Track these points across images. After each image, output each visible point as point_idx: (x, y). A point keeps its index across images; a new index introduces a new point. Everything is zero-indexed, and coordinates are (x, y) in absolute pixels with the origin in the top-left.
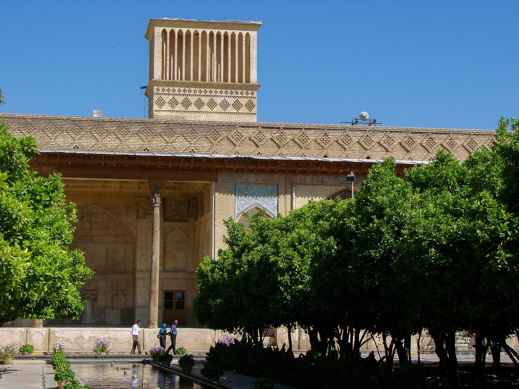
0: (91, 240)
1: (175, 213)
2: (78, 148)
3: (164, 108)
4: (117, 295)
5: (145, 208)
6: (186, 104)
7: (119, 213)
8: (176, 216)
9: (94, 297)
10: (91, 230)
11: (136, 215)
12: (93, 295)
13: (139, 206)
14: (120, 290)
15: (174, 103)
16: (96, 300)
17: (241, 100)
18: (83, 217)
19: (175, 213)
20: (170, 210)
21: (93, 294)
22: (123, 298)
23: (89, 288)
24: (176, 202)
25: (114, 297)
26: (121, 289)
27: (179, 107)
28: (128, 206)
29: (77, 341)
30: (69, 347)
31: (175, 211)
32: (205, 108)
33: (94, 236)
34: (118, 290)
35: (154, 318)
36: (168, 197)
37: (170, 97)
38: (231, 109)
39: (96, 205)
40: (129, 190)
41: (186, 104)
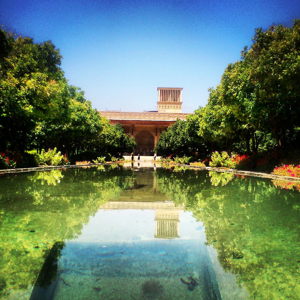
3: (161, 108)
6: (165, 107)
15: (163, 107)
16: (146, 151)
17: (178, 106)
27: (164, 108)
32: (170, 108)
37: (162, 105)
38: (176, 108)
41: (165, 107)
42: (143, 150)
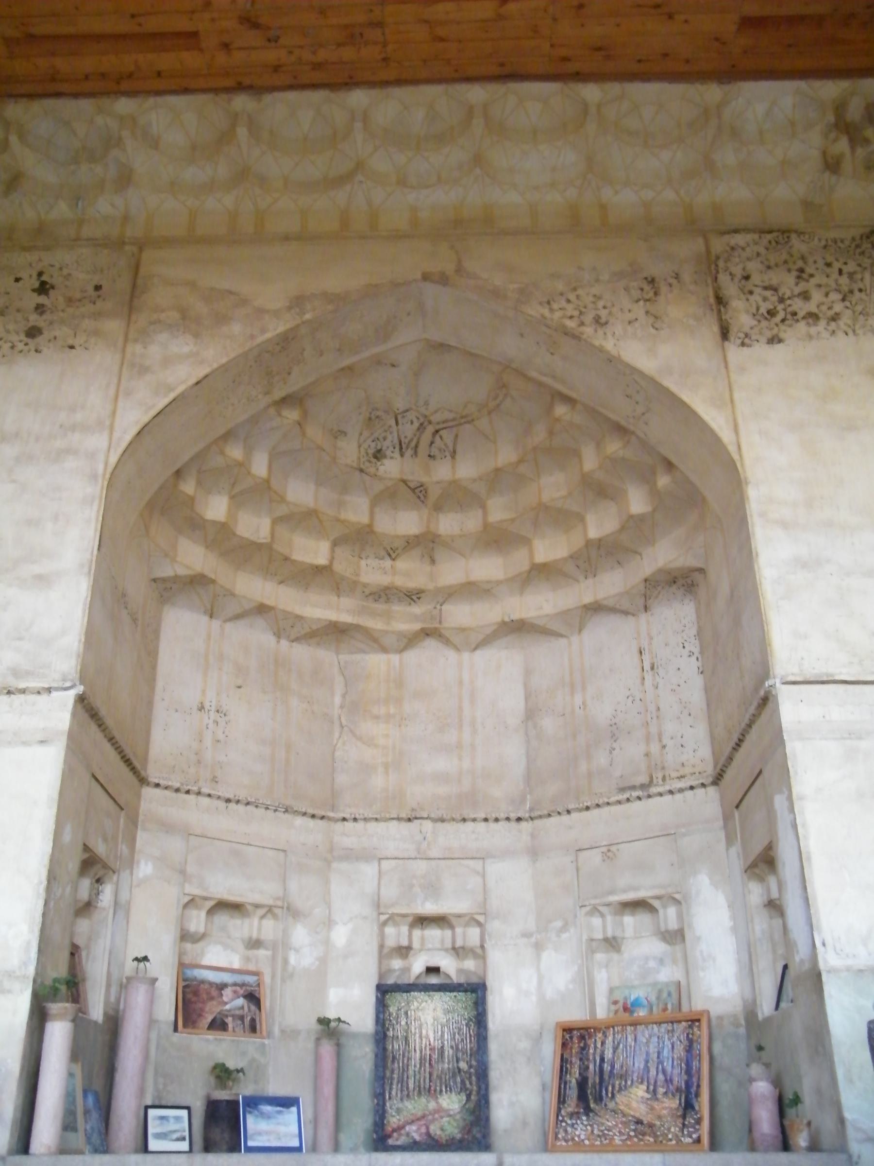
4: (612, 944)
5: (766, 288)
7: (597, 320)
9: (470, 964)
10: (433, 561)
11: (716, 329)
12: (458, 951)
13: (723, 278)
18: (378, 455)
21: (459, 943)
22: (661, 962)
23: (430, 908)
25: (600, 957)
28: (652, 281)
40: (648, 195)
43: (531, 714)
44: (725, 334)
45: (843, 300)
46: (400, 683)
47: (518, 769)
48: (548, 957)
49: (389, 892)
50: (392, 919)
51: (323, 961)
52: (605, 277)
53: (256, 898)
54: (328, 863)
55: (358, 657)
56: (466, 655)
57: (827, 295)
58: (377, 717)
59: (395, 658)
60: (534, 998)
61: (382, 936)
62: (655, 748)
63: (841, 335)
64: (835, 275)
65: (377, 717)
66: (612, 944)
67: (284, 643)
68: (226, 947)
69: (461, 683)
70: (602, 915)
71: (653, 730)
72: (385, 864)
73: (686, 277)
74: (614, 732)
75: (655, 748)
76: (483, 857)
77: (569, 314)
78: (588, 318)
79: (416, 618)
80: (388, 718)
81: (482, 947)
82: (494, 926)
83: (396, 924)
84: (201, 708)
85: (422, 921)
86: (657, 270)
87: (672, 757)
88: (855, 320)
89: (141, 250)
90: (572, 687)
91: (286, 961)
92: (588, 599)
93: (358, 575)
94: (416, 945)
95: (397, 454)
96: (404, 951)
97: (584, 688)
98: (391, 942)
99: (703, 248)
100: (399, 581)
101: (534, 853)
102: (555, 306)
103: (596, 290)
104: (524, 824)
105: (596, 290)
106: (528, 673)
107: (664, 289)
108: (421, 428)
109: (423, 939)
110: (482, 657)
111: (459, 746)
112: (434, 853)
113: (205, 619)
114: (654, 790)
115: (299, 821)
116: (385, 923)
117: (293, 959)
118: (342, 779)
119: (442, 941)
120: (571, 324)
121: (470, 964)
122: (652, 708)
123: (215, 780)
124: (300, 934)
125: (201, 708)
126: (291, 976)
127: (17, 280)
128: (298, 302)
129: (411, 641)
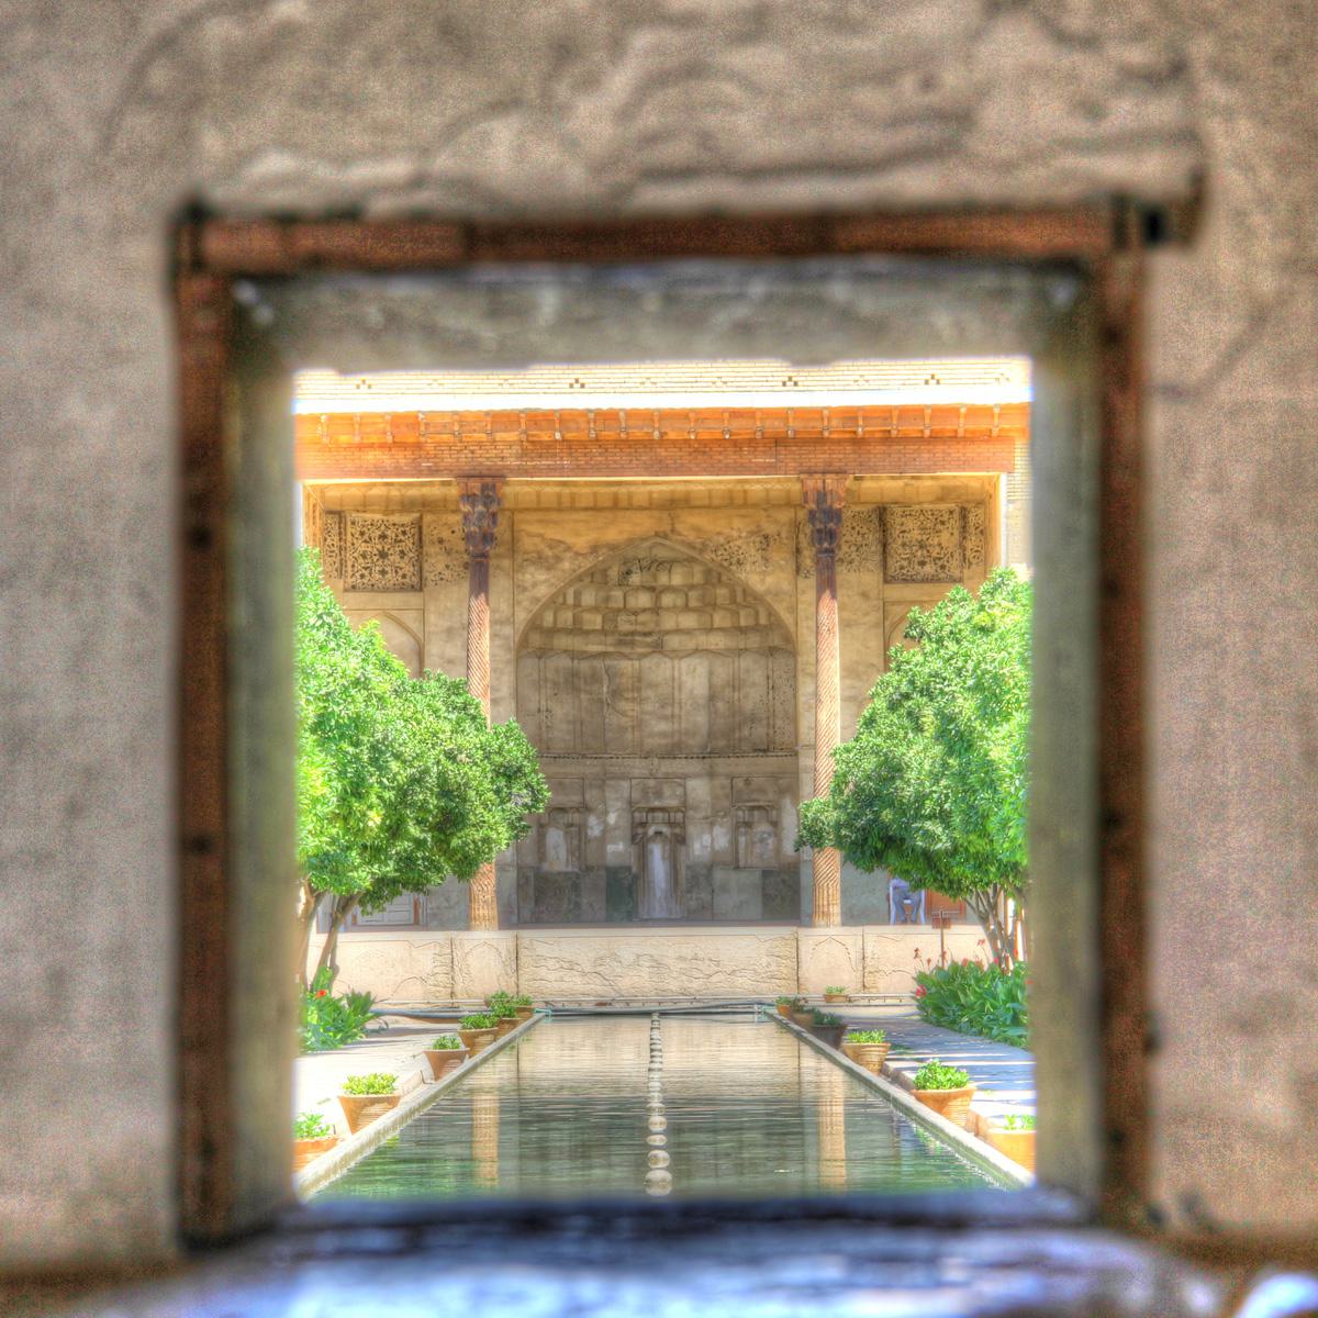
0: (658, 648)
1: (919, 553)
2: (583, 386)
4: (748, 825)
8: (922, 564)
9: (678, 830)
11: (794, 567)
12: (671, 824)
13: (801, 536)
14: (759, 808)
18: (628, 573)
19: (919, 553)
20: (904, 545)
21: (672, 820)
22: (769, 834)
23: (657, 804)
24: (922, 518)
25: (742, 830)
26: (761, 803)
28: (766, 537)
29: (599, 969)
30: (576, 987)
31: (921, 547)
33: (668, 632)
34: (752, 809)
35: (828, 895)
36: (896, 503)
39: (665, 536)
42: (639, 840)
43: (712, 698)
44: (798, 570)
45: (857, 550)
46: (640, 680)
47: (704, 730)
48: (718, 830)
49: (636, 795)
50: (639, 810)
51: (604, 832)
52: (744, 534)
53: (571, 804)
54: (604, 781)
55: (616, 662)
56: (676, 662)
57: (850, 548)
58: (627, 699)
59: (636, 663)
60: (709, 849)
61: (633, 818)
62: (771, 732)
63: (852, 571)
64: (855, 536)
65: (627, 699)
66: (748, 825)
67: (576, 662)
68: (557, 828)
69: (673, 679)
70: (744, 811)
71: (771, 722)
72: (634, 782)
73: (784, 535)
74: (753, 719)
75: (771, 732)
76: (685, 777)
77: (725, 557)
78: (734, 560)
79: (648, 645)
80: (634, 699)
81: (684, 822)
82: (691, 813)
83: (640, 812)
84: (539, 711)
85: (653, 810)
86: (770, 529)
87: (778, 739)
88: (861, 563)
89: (513, 513)
90: (734, 687)
91: (586, 834)
92: (742, 646)
93: (616, 627)
94: (650, 821)
95: (639, 571)
96: (644, 824)
97: (739, 689)
98: (637, 820)
99: (793, 515)
100: (639, 628)
101: (711, 775)
102: (719, 553)
103: (739, 543)
104: (705, 760)
105: (739, 543)
106: (711, 673)
107: (772, 542)
108: (652, 562)
109: (653, 817)
110: (684, 664)
111: (673, 716)
112: (659, 775)
113: (537, 660)
114: (769, 754)
115: (588, 762)
116: (633, 812)
117: (589, 832)
118: (609, 735)
119: (663, 819)
120: (726, 564)
121: (678, 830)
122: (771, 710)
123: (548, 748)
124: (592, 820)
125: (539, 711)
126: (589, 841)
127: (453, 532)
128: (594, 549)
129: (645, 655)
